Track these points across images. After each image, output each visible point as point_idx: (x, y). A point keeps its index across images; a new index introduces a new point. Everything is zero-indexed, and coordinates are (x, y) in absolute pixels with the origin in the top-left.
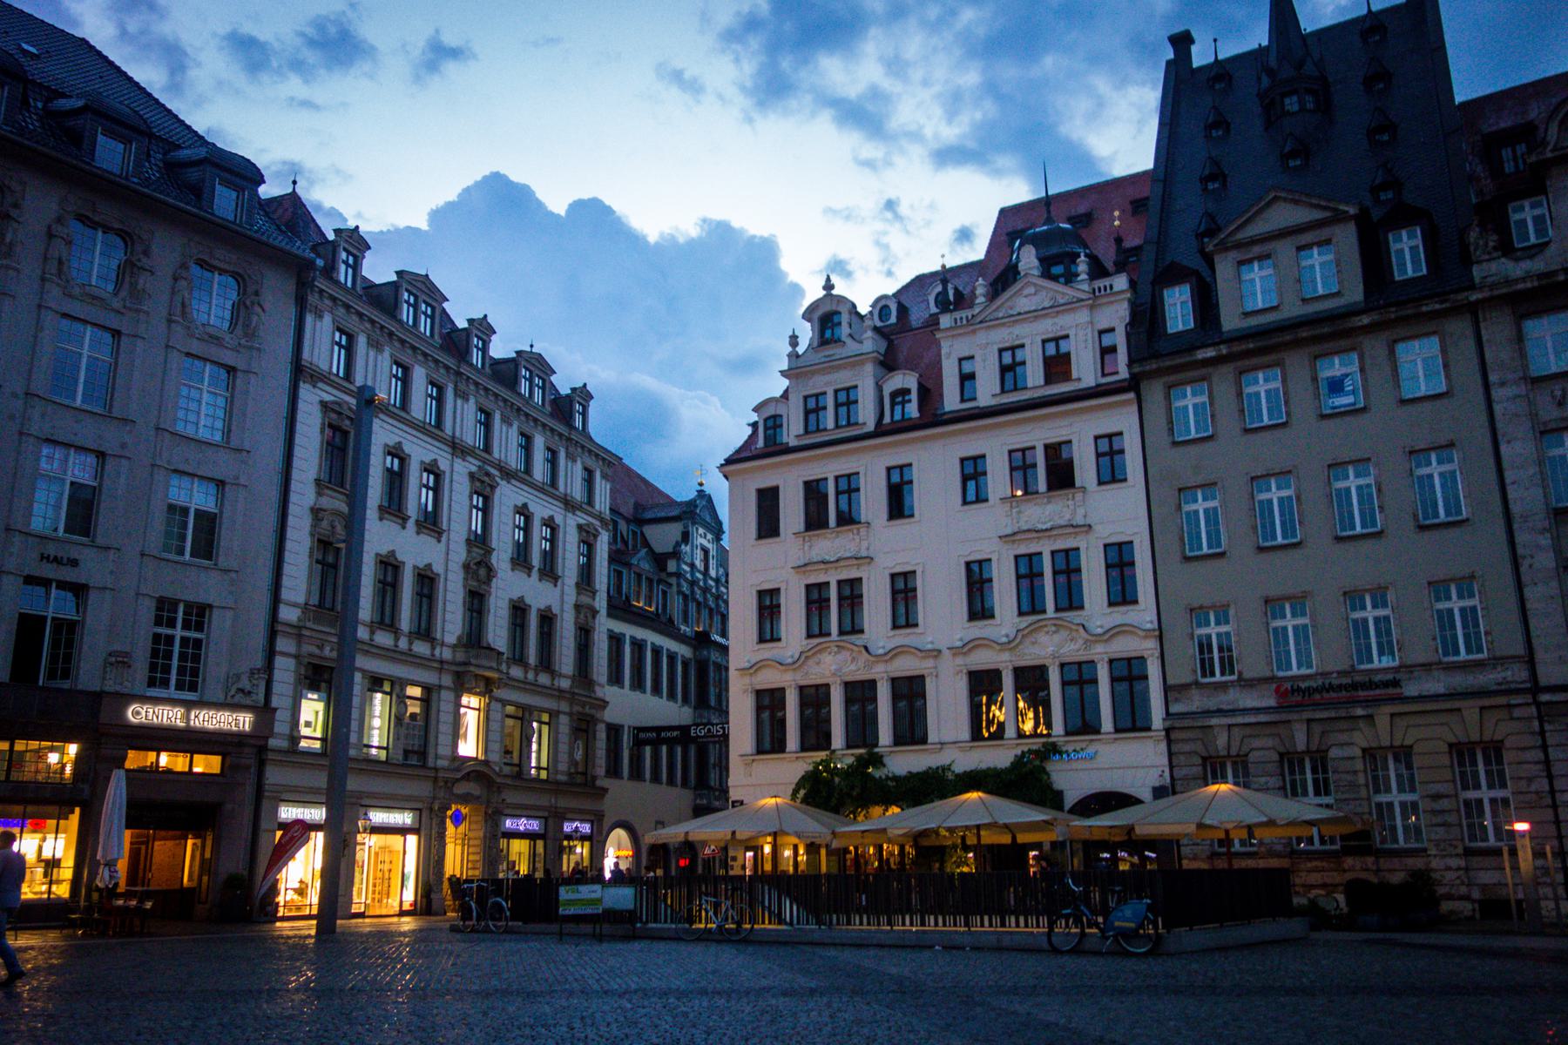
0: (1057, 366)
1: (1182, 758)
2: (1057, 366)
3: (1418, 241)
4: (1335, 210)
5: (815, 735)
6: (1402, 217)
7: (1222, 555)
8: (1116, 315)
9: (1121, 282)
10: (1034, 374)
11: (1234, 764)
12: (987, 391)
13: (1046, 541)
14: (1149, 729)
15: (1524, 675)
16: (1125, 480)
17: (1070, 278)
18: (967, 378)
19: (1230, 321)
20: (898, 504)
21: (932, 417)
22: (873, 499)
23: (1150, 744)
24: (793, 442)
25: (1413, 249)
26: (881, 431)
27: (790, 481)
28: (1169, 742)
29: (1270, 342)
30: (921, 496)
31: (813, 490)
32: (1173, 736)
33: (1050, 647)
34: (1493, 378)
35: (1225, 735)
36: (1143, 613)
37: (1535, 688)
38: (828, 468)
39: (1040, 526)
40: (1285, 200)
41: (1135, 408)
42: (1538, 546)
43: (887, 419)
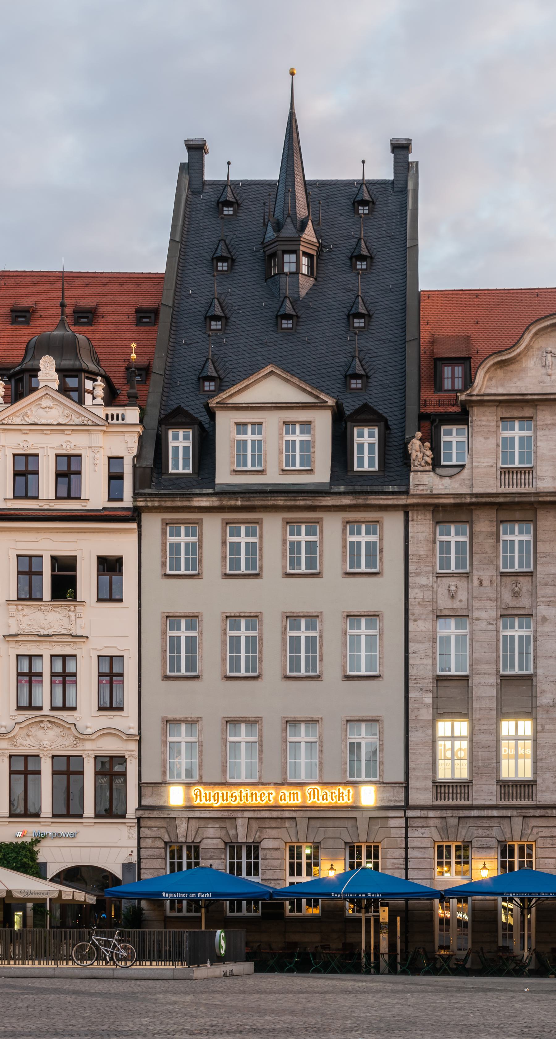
1: (149, 841)
3: (375, 440)
4: (317, 397)
6: (366, 415)
7: (197, 677)
11: (189, 848)
13: (46, 645)
14: (123, 816)
15: (402, 796)
16: (121, 600)
19: (224, 476)
23: (123, 828)
25: (371, 446)
28: (139, 827)
29: (252, 501)
32: (142, 824)
33: (47, 742)
34: (412, 568)
35: (184, 825)
36: (126, 721)
37: (407, 806)
39: (43, 632)
40: (279, 376)
41: (136, 536)
42: (422, 703)
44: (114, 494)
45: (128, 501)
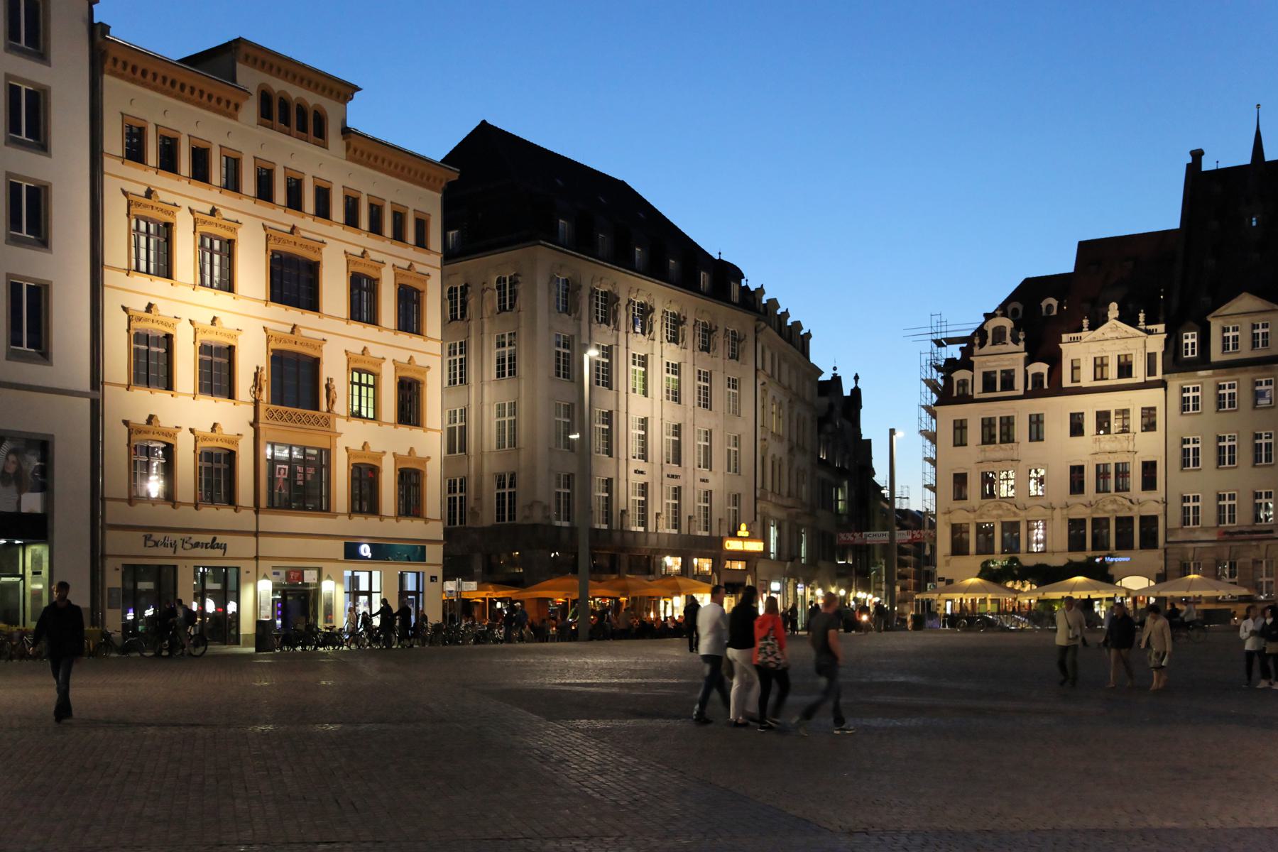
0: (1125, 369)
2: (1125, 369)
5: (986, 547)
8: (1156, 343)
9: (1161, 327)
10: (1112, 371)
12: (1086, 379)
17: (1133, 323)
18: (1075, 368)
19: (1216, 354)
20: (1036, 433)
21: (1057, 389)
22: (1021, 429)
24: (976, 396)
26: (1027, 395)
27: (973, 414)
30: (1049, 428)
31: (987, 424)
38: (997, 410)
43: (1030, 388)
44: (1151, 370)
45: (1159, 376)
